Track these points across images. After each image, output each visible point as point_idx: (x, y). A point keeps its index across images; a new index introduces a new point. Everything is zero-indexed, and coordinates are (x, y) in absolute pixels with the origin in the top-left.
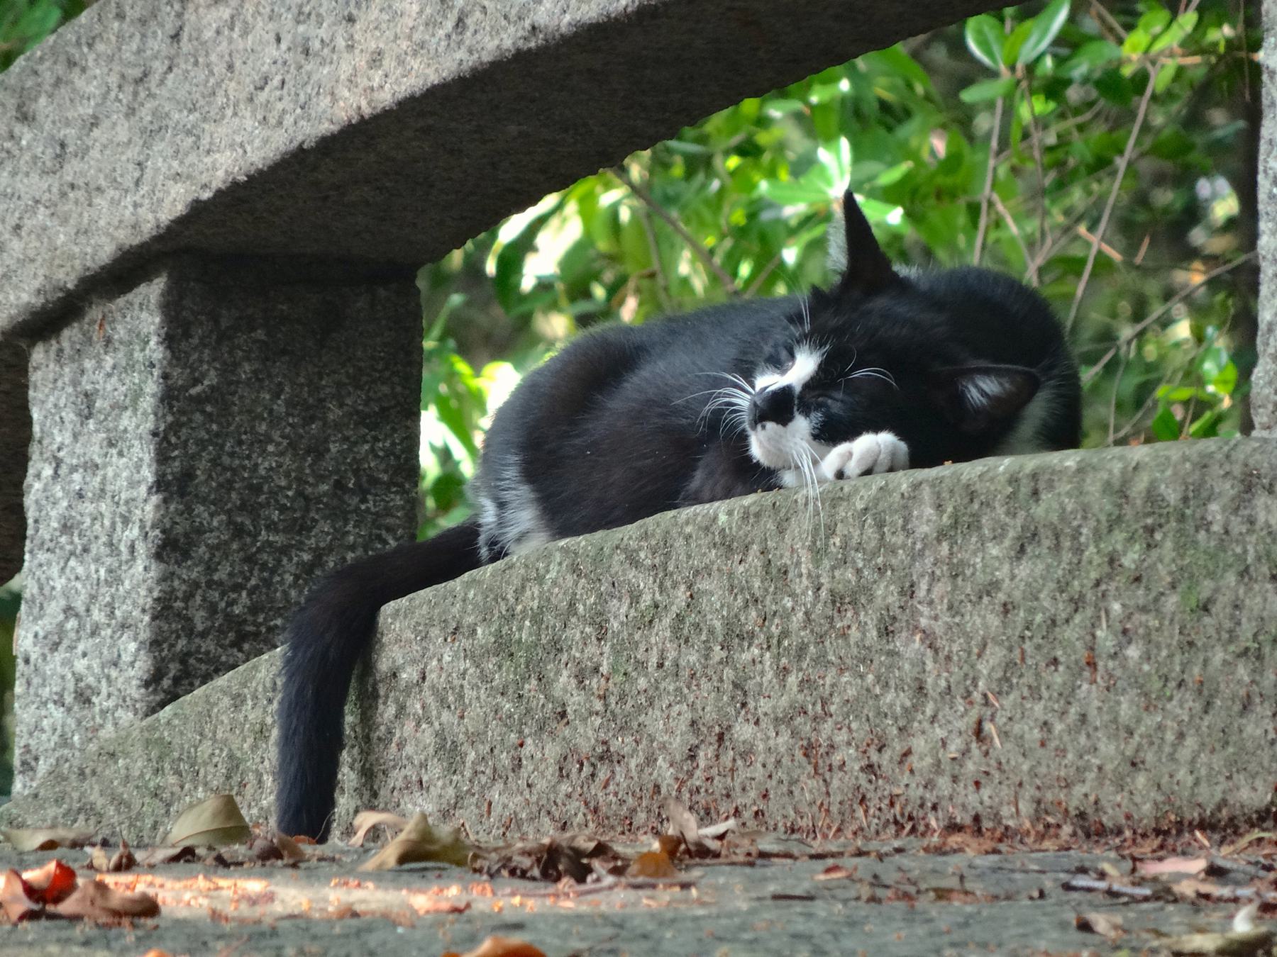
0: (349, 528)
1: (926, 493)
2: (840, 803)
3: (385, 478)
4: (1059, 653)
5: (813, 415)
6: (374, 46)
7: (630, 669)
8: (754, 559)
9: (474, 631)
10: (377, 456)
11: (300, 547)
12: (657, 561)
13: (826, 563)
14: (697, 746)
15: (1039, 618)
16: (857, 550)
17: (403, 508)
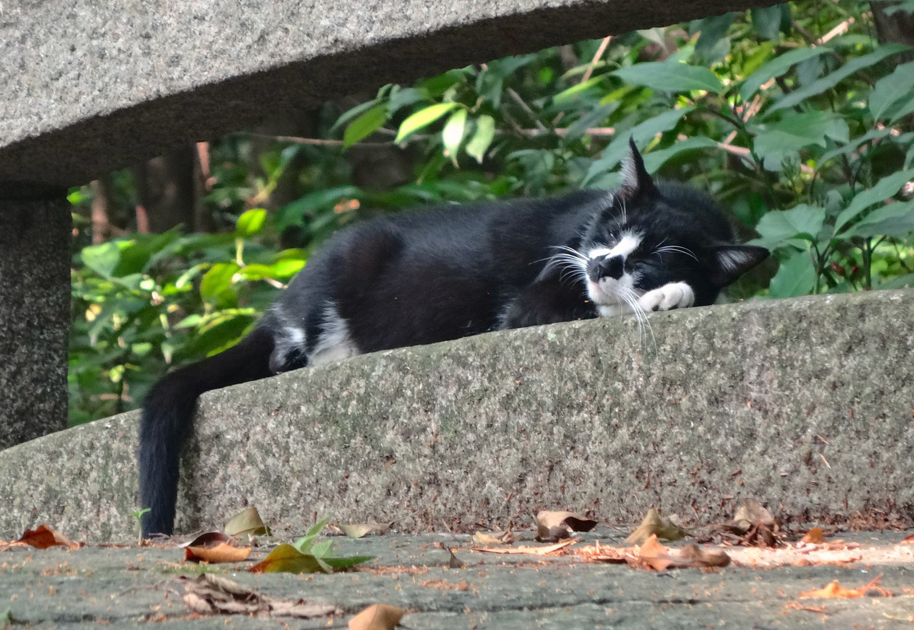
0: (35, 350)
1: (754, 317)
2: (672, 505)
3: (53, 319)
4: (886, 411)
5: (634, 273)
6: (172, 52)
7: (460, 429)
8: (584, 358)
9: (299, 408)
10: (49, 306)
11: (9, 362)
12: (486, 362)
13: (658, 361)
14: (526, 474)
15: (868, 390)
16: (687, 353)
17: (63, 337)
